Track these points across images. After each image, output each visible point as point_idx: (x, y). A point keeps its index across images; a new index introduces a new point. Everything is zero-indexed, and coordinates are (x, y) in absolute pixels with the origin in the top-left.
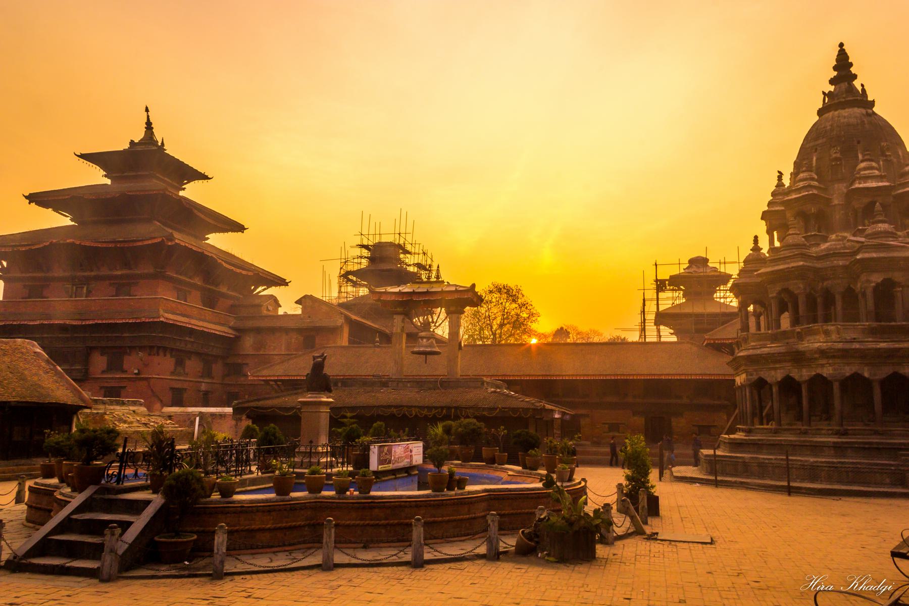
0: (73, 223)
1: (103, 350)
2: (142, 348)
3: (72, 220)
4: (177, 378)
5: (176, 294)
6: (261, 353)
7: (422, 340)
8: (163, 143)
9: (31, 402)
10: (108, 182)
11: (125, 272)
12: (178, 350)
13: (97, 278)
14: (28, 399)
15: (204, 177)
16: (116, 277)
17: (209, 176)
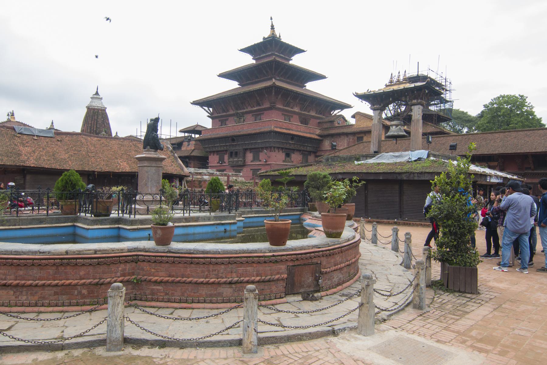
0: (239, 86)
1: (251, 149)
2: (266, 148)
3: (238, 84)
5: (284, 118)
7: (392, 128)
8: (280, 36)
10: (254, 62)
12: (286, 149)
15: (303, 51)
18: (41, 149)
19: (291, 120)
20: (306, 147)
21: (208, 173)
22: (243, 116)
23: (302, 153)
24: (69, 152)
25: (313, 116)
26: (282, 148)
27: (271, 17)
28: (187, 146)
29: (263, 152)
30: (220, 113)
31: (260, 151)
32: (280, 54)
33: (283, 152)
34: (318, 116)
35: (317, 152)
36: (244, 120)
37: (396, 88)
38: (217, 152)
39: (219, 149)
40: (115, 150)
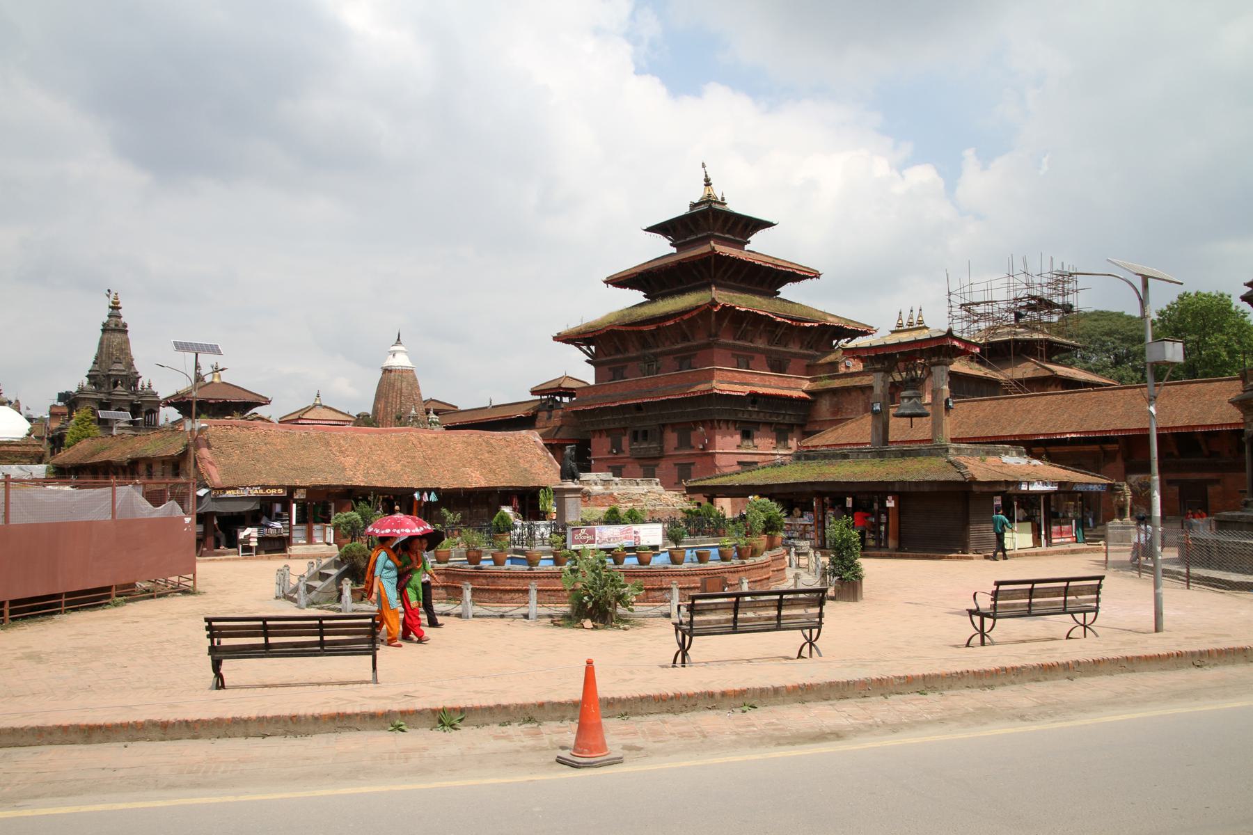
0: (647, 299)
1: (673, 427)
2: (704, 423)
3: (644, 296)
4: (744, 451)
5: (736, 362)
6: (839, 418)
7: (903, 401)
8: (723, 199)
9: (517, 487)
10: (674, 250)
13: (663, 354)
14: (514, 484)
15: (768, 225)
16: (679, 351)
19: (751, 366)
20: (782, 416)
21: (601, 480)
22: (657, 361)
23: (775, 430)
28: (548, 419)
29: (698, 430)
30: (611, 355)
31: (692, 429)
33: (736, 429)
34: (806, 352)
35: (806, 425)
37: (905, 337)
38: (608, 432)
39: (612, 426)
40: (460, 453)
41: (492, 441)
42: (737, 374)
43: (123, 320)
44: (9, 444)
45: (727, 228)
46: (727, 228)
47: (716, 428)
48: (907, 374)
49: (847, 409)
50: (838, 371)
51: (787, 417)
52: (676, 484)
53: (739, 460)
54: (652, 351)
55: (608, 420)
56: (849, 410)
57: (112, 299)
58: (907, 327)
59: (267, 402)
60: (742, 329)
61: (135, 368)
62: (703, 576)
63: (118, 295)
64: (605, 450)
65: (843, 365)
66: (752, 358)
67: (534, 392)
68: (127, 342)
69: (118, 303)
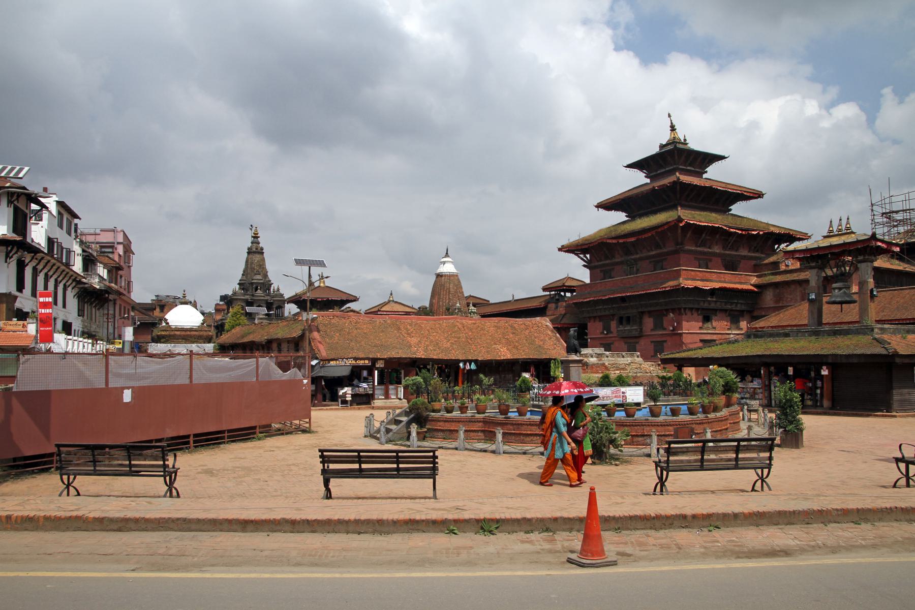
0: (628, 218)
2: (673, 310)
3: (626, 216)
4: (705, 332)
5: (698, 264)
6: (780, 305)
7: (834, 291)
8: (685, 140)
9: (532, 359)
10: (648, 181)
11: (658, 251)
12: (703, 309)
13: (641, 259)
15: (721, 158)
16: (653, 256)
17: (726, 156)
18: (425, 339)
19: (710, 265)
21: (595, 354)
22: (637, 264)
23: (729, 315)
24: (450, 340)
25: (745, 256)
26: (697, 310)
27: (669, 114)
28: (555, 309)
29: (668, 316)
30: (601, 260)
32: (687, 167)
34: (753, 254)
36: (638, 270)
37: (835, 241)
38: (601, 318)
39: (603, 313)
40: (492, 334)
41: (515, 325)
42: (698, 273)
43: (261, 245)
44: (191, 330)
45: (689, 162)
46: (689, 162)
47: (682, 314)
48: (837, 270)
49: (787, 298)
50: (779, 269)
51: (739, 305)
52: (652, 356)
53: (701, 339)
54: (633, 257)
55: (601, 309)
56: (789, 299)
57: (253, 231)
58: (837, 232)
59: (355, 299)
60: (702, 239)
61: (268, 278)
62: (675, 427)
63: (257, 229)
64: (598, 331)
65: (783, 264)
66: (711, 260)
67: (544, 289)
68: (263, 260)
69: (257, 234)
